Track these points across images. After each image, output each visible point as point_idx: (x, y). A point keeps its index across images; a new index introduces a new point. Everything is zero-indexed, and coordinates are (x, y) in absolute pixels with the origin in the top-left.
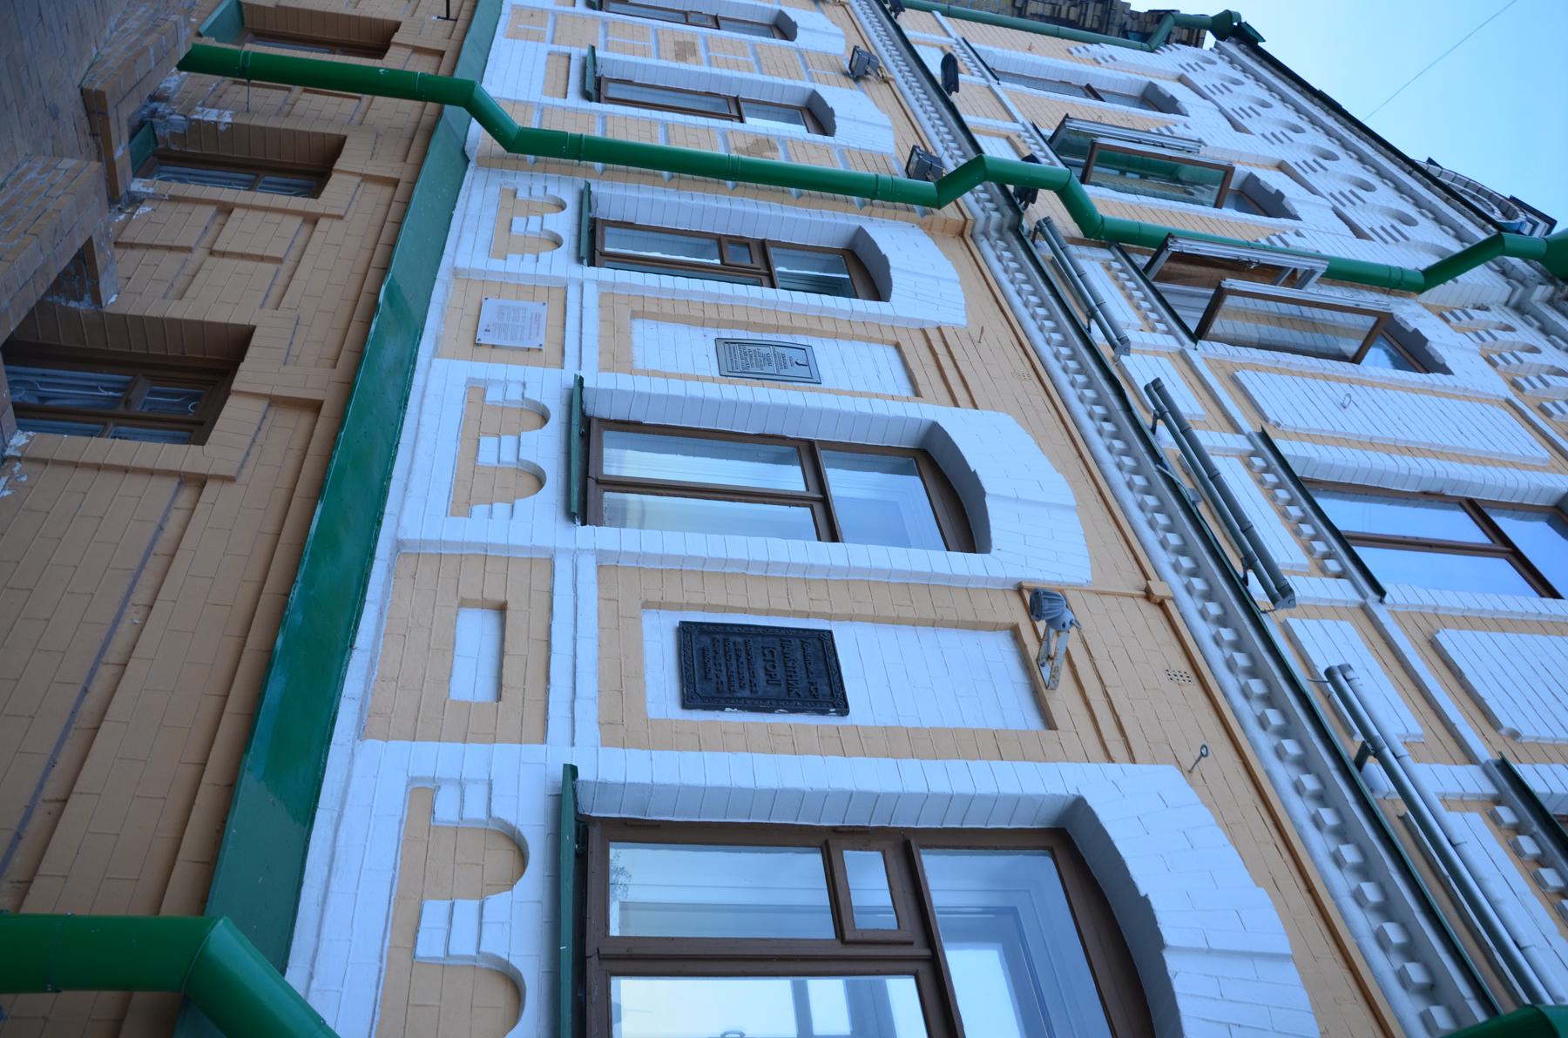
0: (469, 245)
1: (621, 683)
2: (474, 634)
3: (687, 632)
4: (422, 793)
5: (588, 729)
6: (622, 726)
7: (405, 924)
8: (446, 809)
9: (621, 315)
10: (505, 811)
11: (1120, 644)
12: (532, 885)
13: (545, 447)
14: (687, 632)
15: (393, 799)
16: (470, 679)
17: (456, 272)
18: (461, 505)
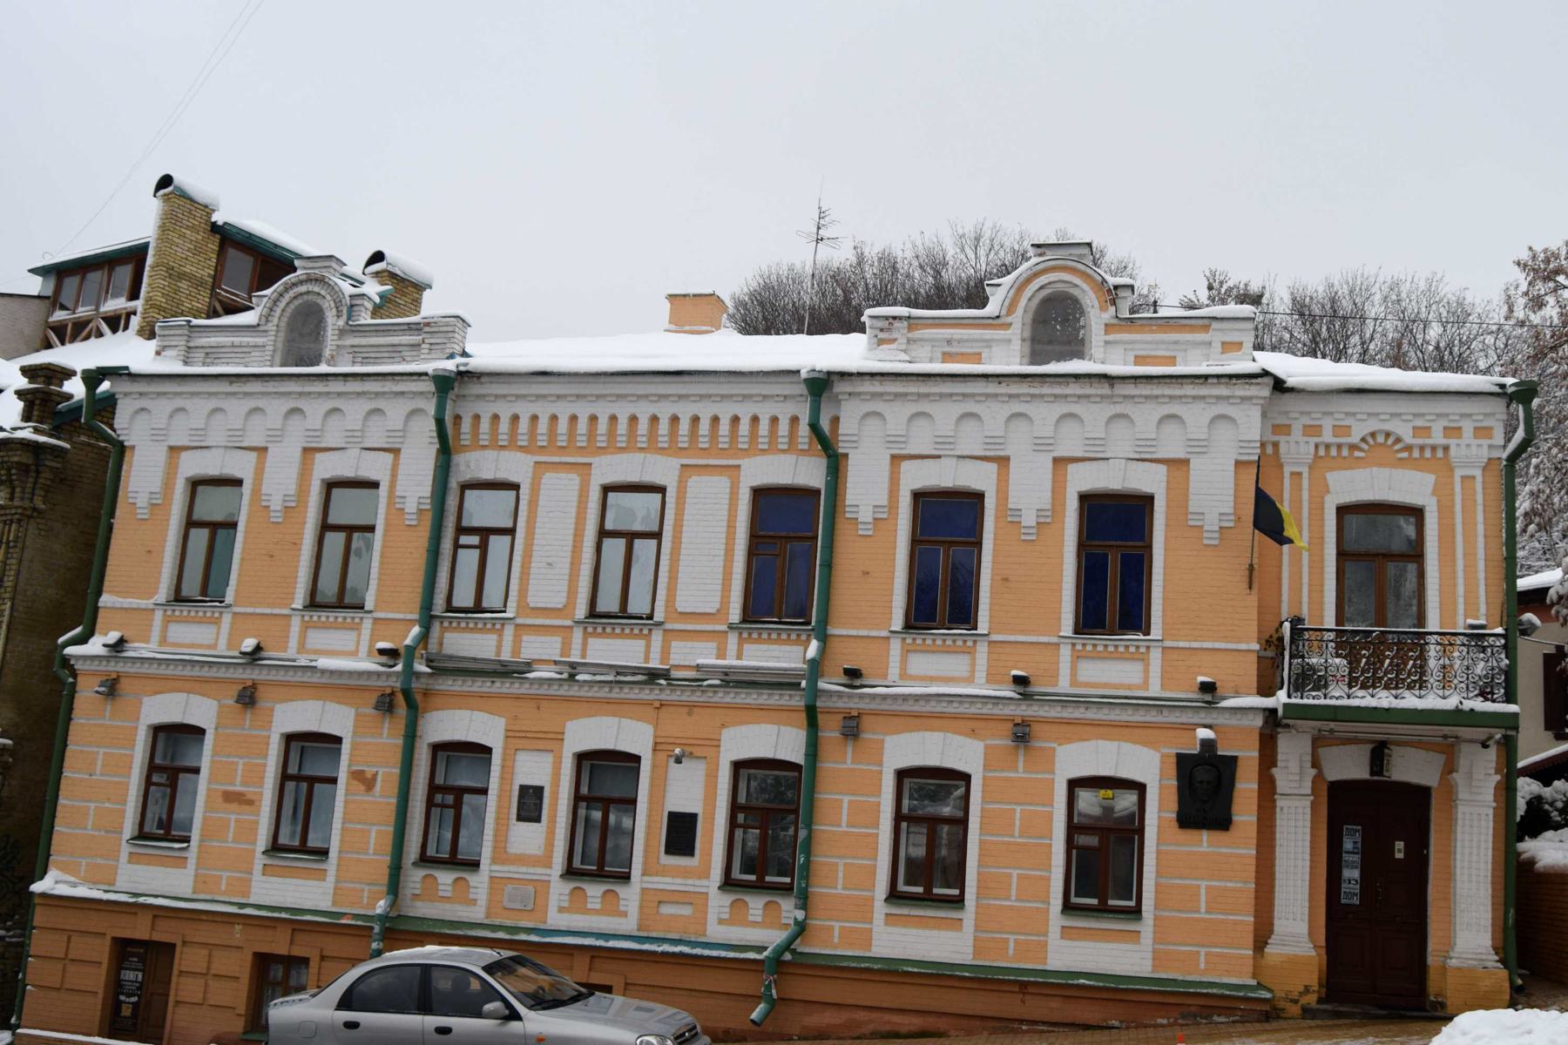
0: (477, 913)
1: (686, 873)
2: (667, 910)
3: (668, 852)
4: (721, 922)
5: (704, 882)
6: (705, 874)
7: (755, 924)
8: (726, 916)
9: (501, 856)
10: (728, 903)
11: (679, 726)
12: (747, 898)
13: (594, 891)
14: (668, 852)
15: (722, 928)
16: (686, 911)
17: (488, 916)
18: (625, 914)
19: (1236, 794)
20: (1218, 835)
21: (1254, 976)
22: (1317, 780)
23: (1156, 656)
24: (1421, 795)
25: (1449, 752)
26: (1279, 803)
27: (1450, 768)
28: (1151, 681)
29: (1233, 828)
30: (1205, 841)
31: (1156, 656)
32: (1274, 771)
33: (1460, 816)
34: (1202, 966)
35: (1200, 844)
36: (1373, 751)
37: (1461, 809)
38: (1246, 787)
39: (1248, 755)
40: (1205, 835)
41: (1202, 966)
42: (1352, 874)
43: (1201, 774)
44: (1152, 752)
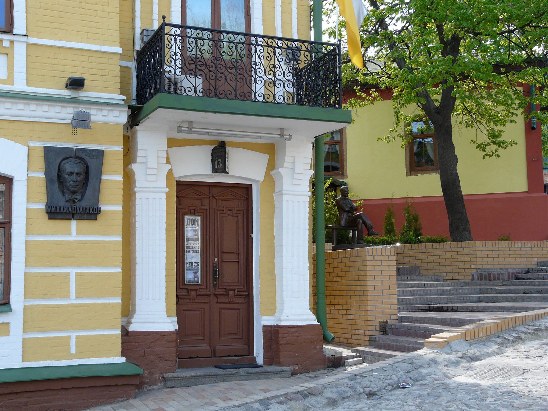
19: (103, 186)
20: (86, 224)
21: (123, 355)
22: (170, 173)
23: (20, 51)
24: (246, 190)
25: (272, 151)
26: (138, 195)
27: (272, 166)
28: (16, 75)
29: (99, 217)
30: (74, 231)
31: (20, 51)
32: (134, 166)
33: (285, 203)
34: (73, 351)
35: (69, 233)
36: (214, 150)
37: (285, 197)
38: (111, 177)
39: (114, 149)
40: (74, 224)
41: (73, 351)
42: (193, 257)
43: (69, 167)
44: (18, 145)
